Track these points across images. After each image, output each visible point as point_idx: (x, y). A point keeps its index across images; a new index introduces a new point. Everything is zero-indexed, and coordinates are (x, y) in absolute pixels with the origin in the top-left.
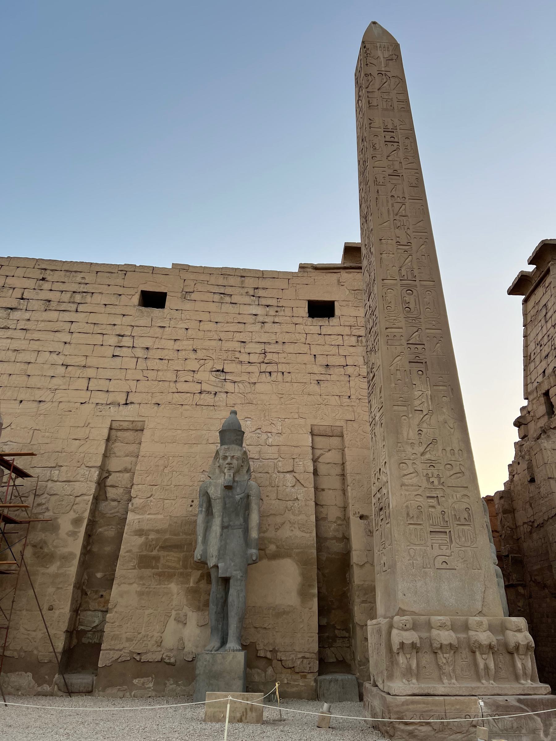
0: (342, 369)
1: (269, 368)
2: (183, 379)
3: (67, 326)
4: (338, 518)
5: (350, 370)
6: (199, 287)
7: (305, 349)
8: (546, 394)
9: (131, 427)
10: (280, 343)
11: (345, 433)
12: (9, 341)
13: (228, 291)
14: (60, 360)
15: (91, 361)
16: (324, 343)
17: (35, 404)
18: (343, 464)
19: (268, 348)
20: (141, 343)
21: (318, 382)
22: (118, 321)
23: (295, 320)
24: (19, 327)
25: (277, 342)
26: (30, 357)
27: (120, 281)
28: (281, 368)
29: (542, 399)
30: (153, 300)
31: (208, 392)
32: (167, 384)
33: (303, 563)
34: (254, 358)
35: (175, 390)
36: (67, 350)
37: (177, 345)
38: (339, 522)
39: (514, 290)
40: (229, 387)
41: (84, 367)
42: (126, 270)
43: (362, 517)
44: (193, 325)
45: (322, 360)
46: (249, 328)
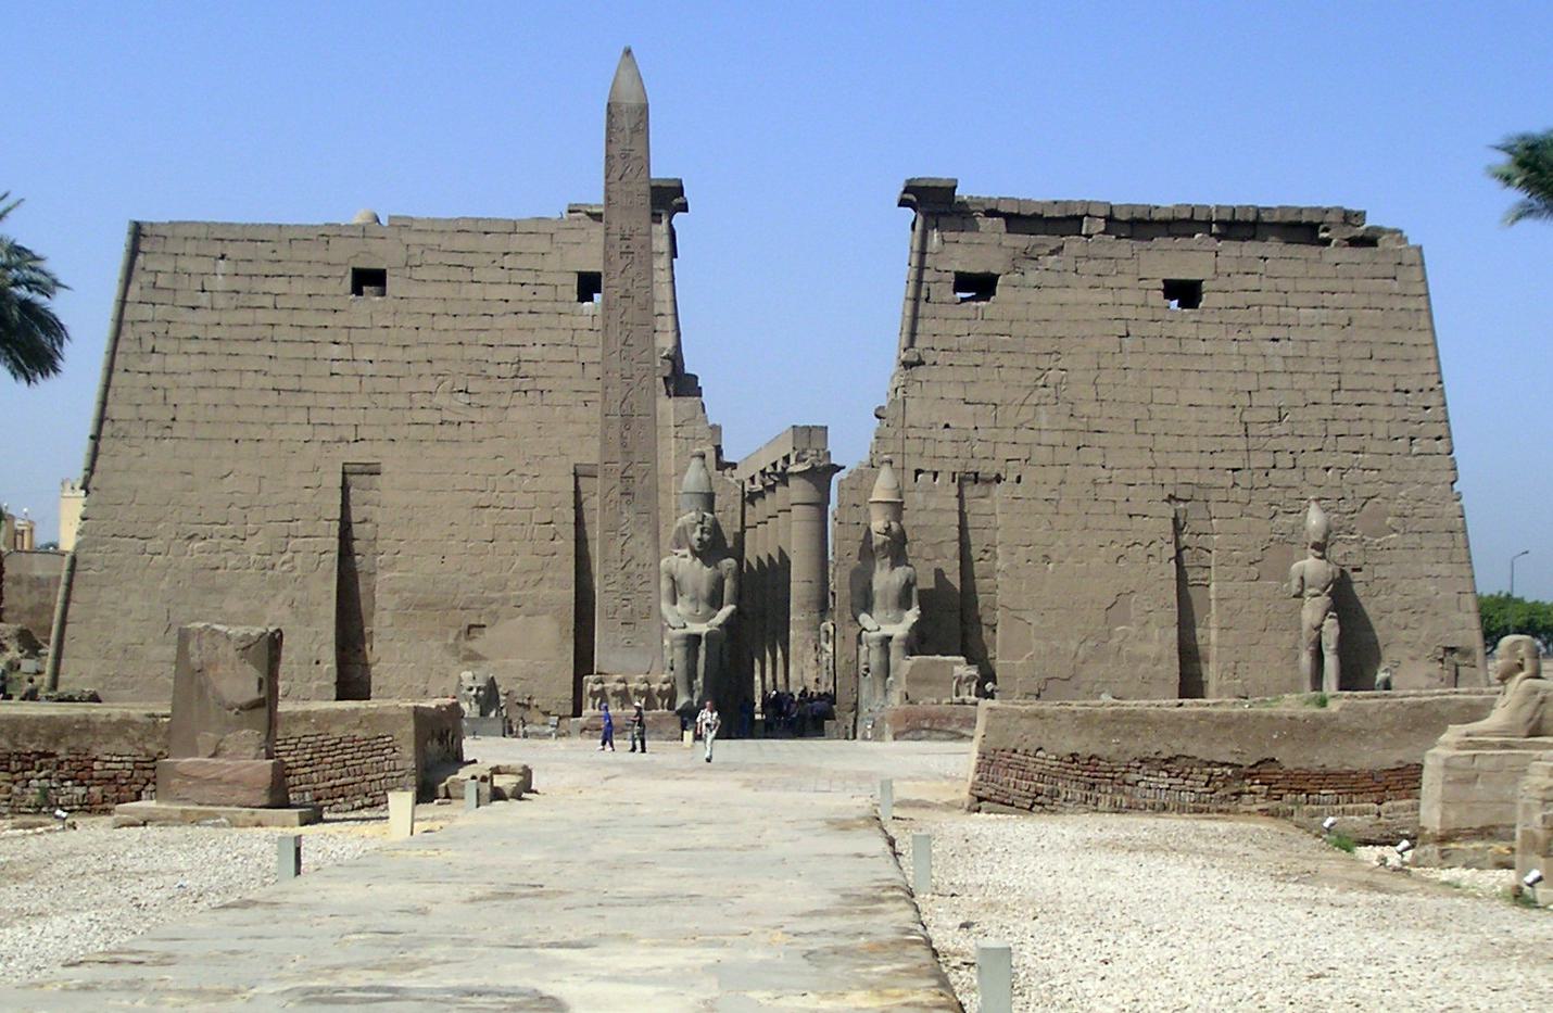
1: (526, 384)
2: (419, 405)
3: (268, 332)
6: (430, 258)
7: (569, 354)
9: (366, 469)
12: (202, 356)
13: (469, 260)
14: (268, 382)
15: (306, 384)
17: (254, 444)
19: (525, 354)
20: (365, 354)
22: (328, 320)
23: (559, 307)
24: (210, 336)
26: (233, 381)
27: (319, 254)
30: (368, 279)
31: (451, 423)
32: (400, 412)
34: (506, 370)
35: (410, 421)
36: (274, 367)
37: (411, 354)
40: (475, 415)
41: (299, 391)
42: (327, 235)
44: (424, 321)
46: (499, 323)
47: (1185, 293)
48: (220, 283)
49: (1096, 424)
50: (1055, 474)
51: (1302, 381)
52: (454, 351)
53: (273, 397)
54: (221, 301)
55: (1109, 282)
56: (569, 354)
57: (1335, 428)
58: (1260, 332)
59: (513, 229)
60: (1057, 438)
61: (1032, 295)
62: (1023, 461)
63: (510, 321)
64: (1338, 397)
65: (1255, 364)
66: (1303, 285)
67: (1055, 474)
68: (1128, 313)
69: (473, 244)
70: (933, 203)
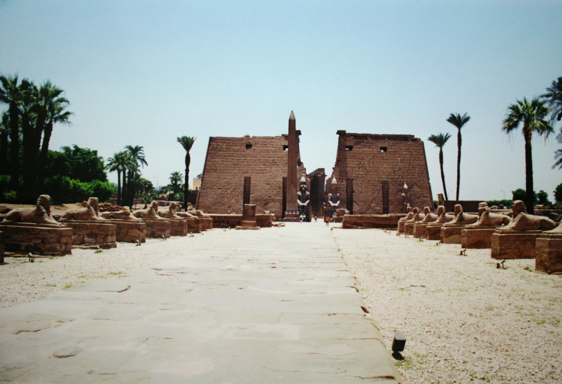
22: (242, 153)
47: (385, 149)
48: (224, 147)
50: (362, 179)
51: (404, 164)
52: (263, 158)
53: (233, 166)
54: (225, 150)
58: (397, 155)
59: (273, 138)
61: (358, 149)
63: (272, 153)
65: (396, 161)
67: (362, 179)
69: (266, 140)
70: (341, 134)
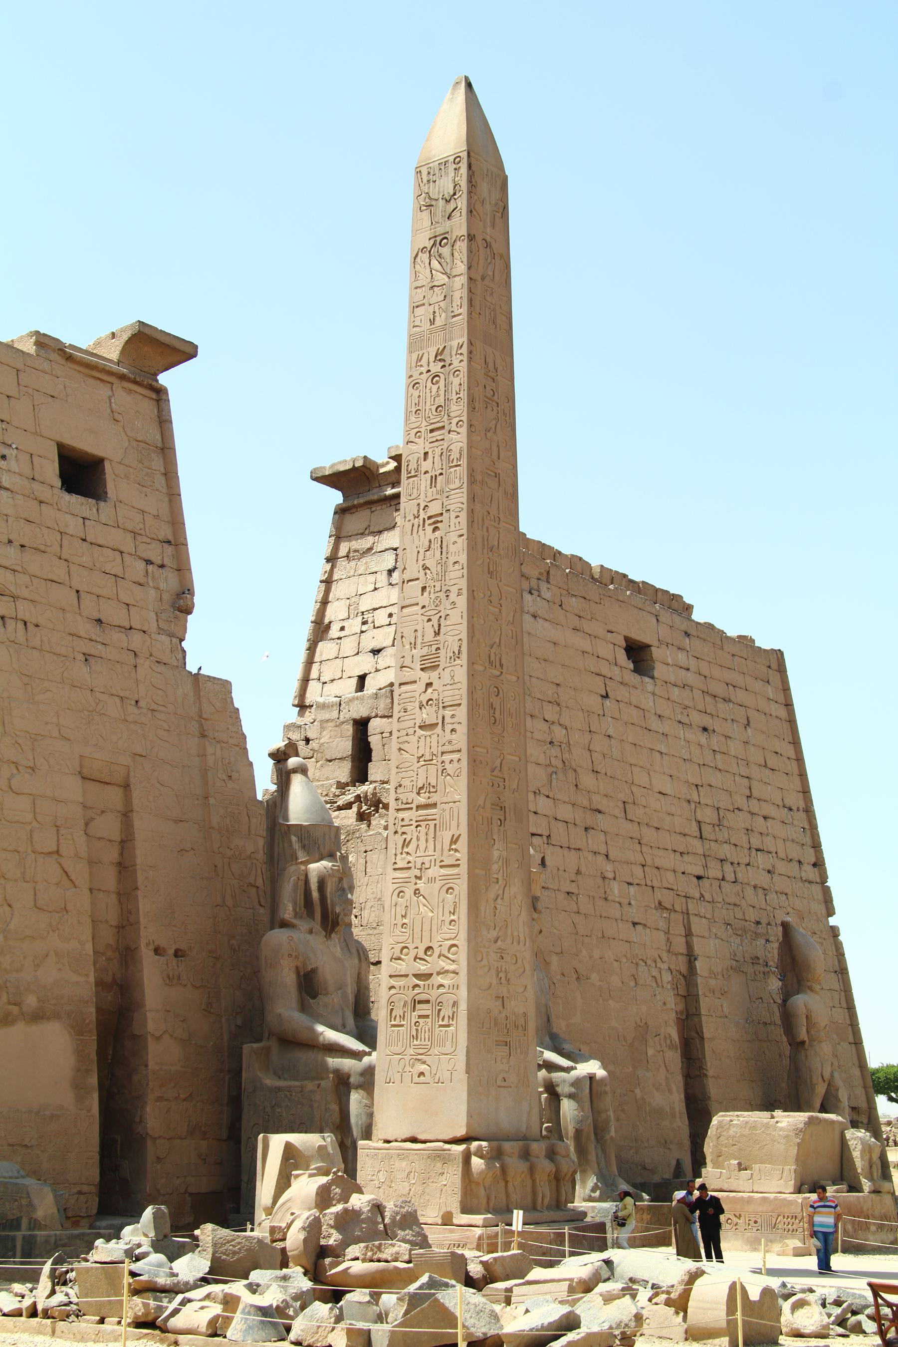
0: (123, 636)
4: (109, 946)
5: (136, 640)
8: (361, 725)
10: (16, 544)
11: (132, 780)
16: (91, 565)
18: (122, 841)
21: (87, 657)
25: (10, 542)
28: (24, 610)
29: (349, 729)
33: (78, 1030)
38: (109, 954)
39: (333, 480)
43: (157, 951)
45: (89, 606)
49: (598, 801)
55: (587, 626)
56: (59, 572)
57: (756, 842)
60: (565, 812)
62: (545, 838)
64: (754, 806)
66: (716, 672)
68: (605, 671)
